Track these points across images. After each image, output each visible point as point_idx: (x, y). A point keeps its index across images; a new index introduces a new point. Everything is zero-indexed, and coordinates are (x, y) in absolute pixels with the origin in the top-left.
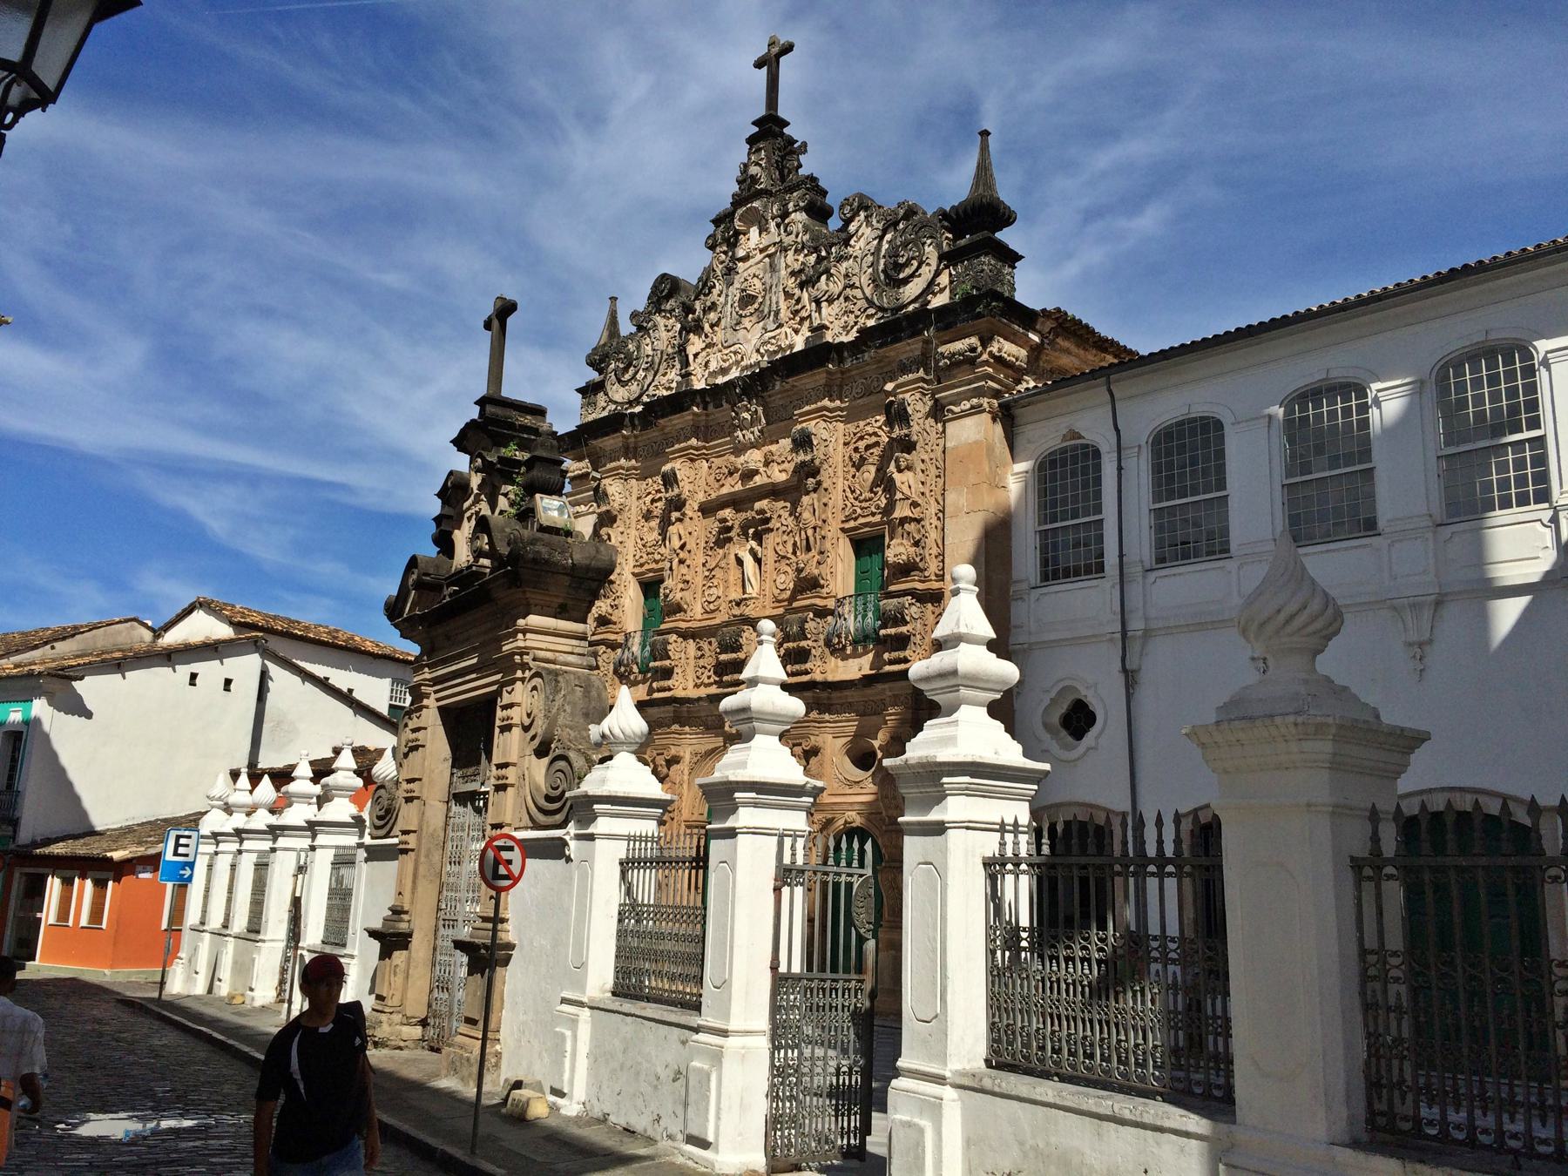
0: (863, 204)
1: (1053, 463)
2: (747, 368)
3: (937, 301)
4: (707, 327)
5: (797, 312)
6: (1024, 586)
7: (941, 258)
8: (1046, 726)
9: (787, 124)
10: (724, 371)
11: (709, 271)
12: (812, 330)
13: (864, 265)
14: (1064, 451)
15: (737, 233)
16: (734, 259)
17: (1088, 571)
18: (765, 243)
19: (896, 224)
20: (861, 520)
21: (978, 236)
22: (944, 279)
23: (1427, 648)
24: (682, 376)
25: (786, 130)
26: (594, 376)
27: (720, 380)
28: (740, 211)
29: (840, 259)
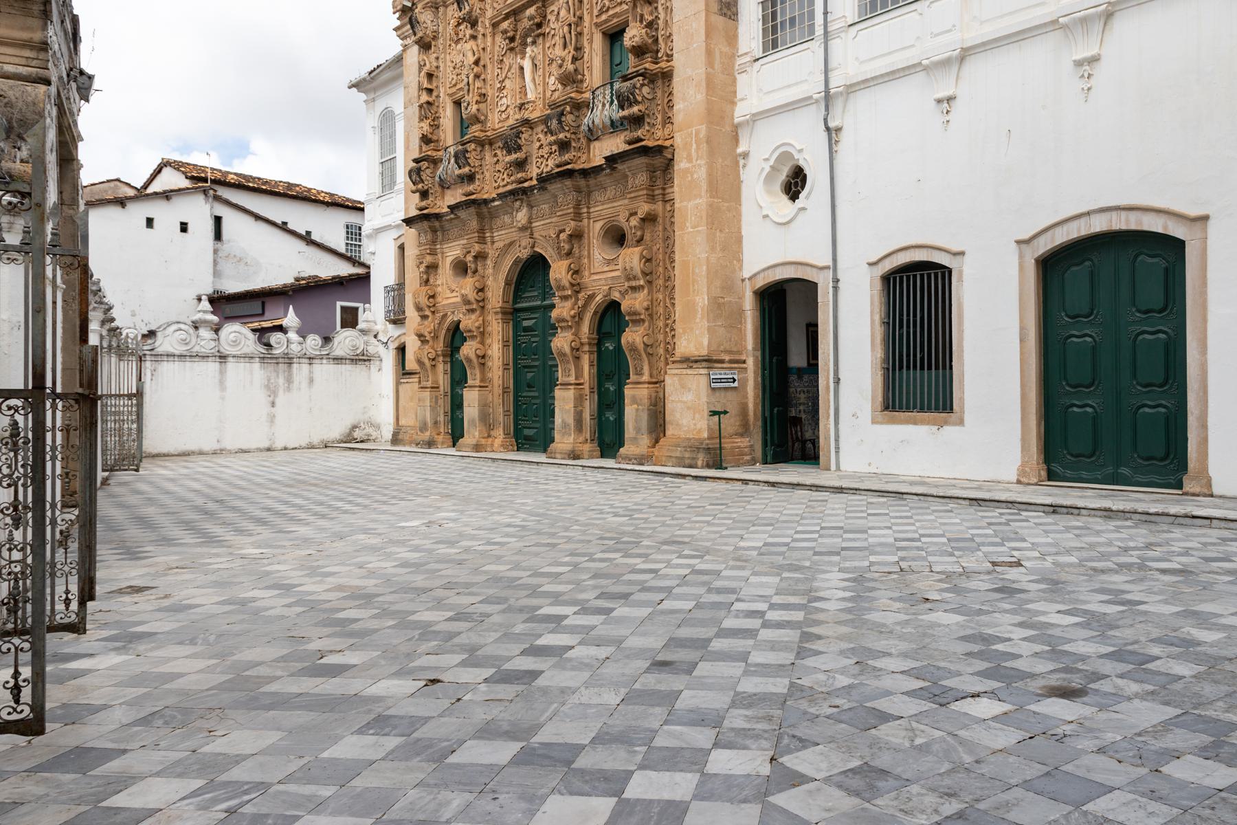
20: (611, 12)
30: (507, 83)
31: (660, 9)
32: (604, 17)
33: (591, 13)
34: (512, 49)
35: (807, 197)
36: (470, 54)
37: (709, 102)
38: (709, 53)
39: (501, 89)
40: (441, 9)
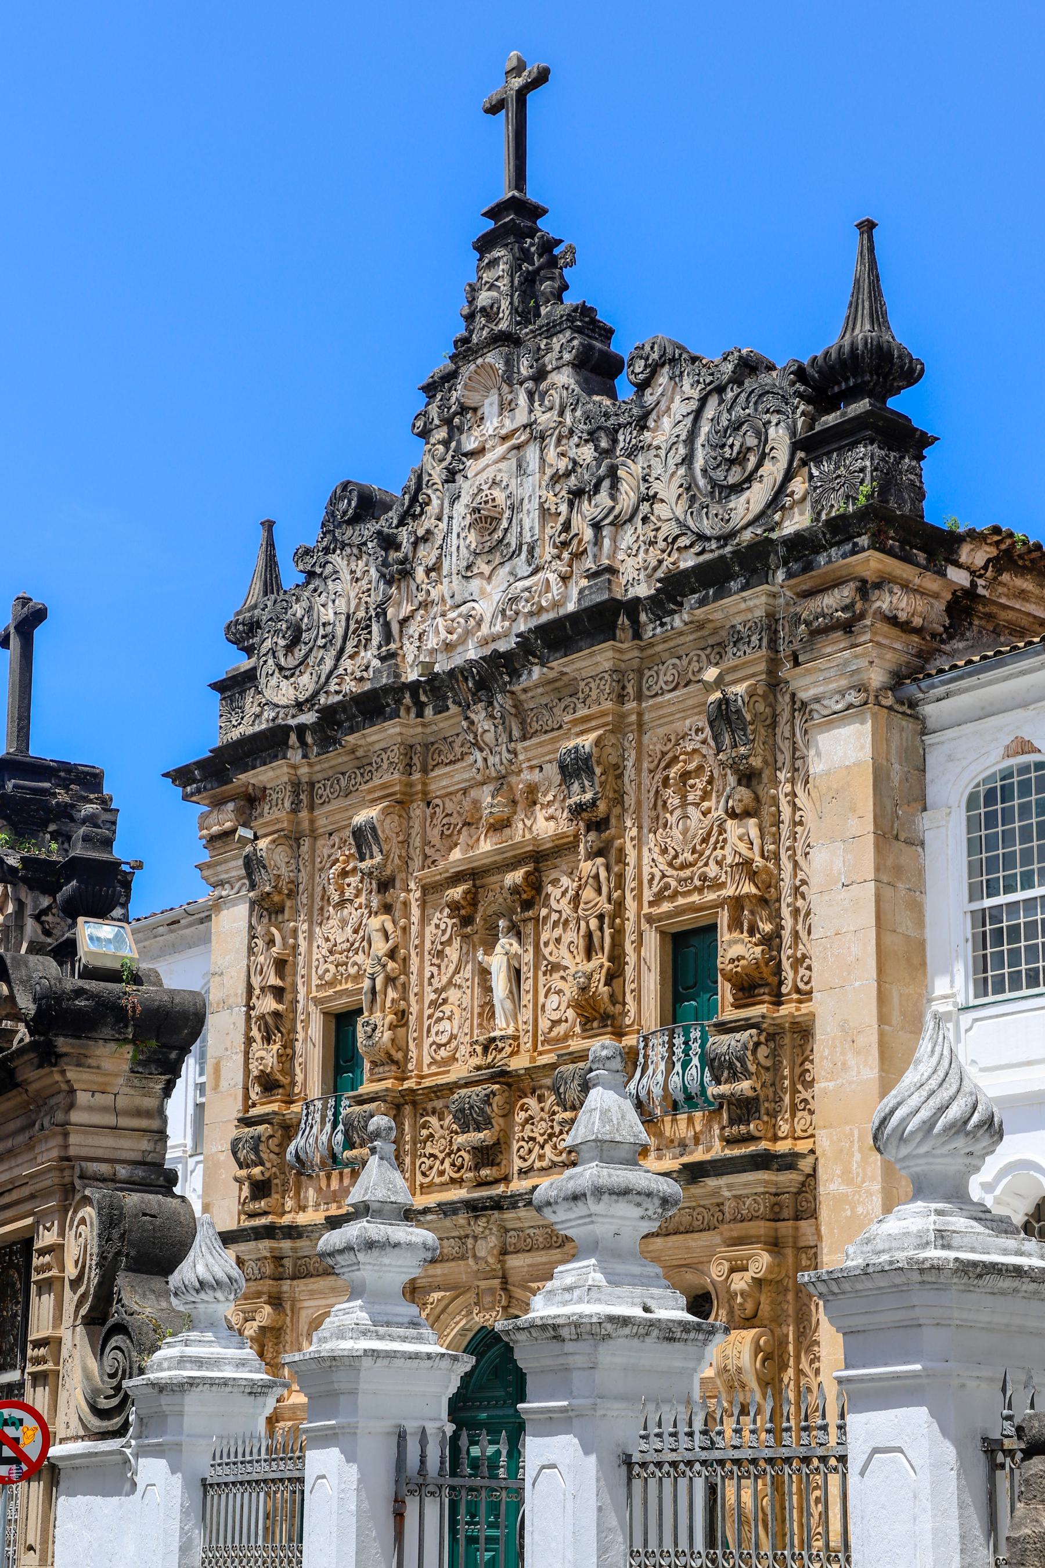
1: (990, 797)
2: (485, 642)
4: (420, 573)
7: (795, 447)
13: (671, 462)
14: (1007, 775)
15: (463, 410)
18: (509, 426)
19: (720, 390)
24: (383, 659)
29: (632, 453)
30: (453, 994)
32: (666, 907)
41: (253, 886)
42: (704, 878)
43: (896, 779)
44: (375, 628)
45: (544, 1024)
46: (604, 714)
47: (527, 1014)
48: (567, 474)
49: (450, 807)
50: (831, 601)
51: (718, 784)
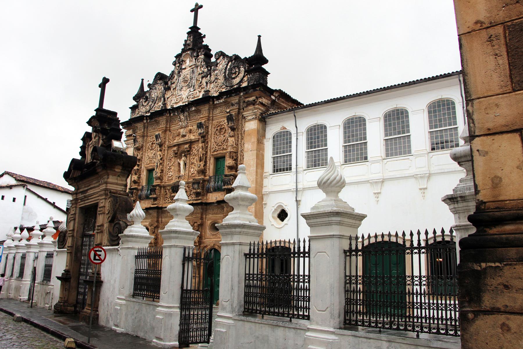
0: (221, 54)
2: (183, 103)
3: (244, 85)
4: (172, 89)
5: (200, 86)
6: (268, 174)
7: (245, 71)
8: (273, 217)
9: (200, 29)
10: (176, 103)
11: (173, 72)
12: (205, 92)
14: (281, 133)
15: (183, 61)
16: (182, 69)
17: (287, 170)
19: (232, 61)
20: (218, 152)
21: (257, 66)
22: (245, 79)
23: (380, 195)
25: (199, 31)
26: (136, 103)
27: (175, 106)
28: (184, 54)
29: (214, 71)
30: (173, 168)
31: (239, 155)
32: (215, 153)
33: (210, 151)
34: (175, 157)
35: (288, 221)
36: (159, 156)
37: (256, 187)
38: (257, 172)
39: (169, 169)
40: (146, 138)
41: (135, 145)
42: (223, 148)
43: (261, 132)
44: (162, 99)
45: (190, 174)
46: (206, 117)
47: (187, 172)
48: (202, 74)
49: (174, 132)
50: (251, 99)
51: (227, 131)
